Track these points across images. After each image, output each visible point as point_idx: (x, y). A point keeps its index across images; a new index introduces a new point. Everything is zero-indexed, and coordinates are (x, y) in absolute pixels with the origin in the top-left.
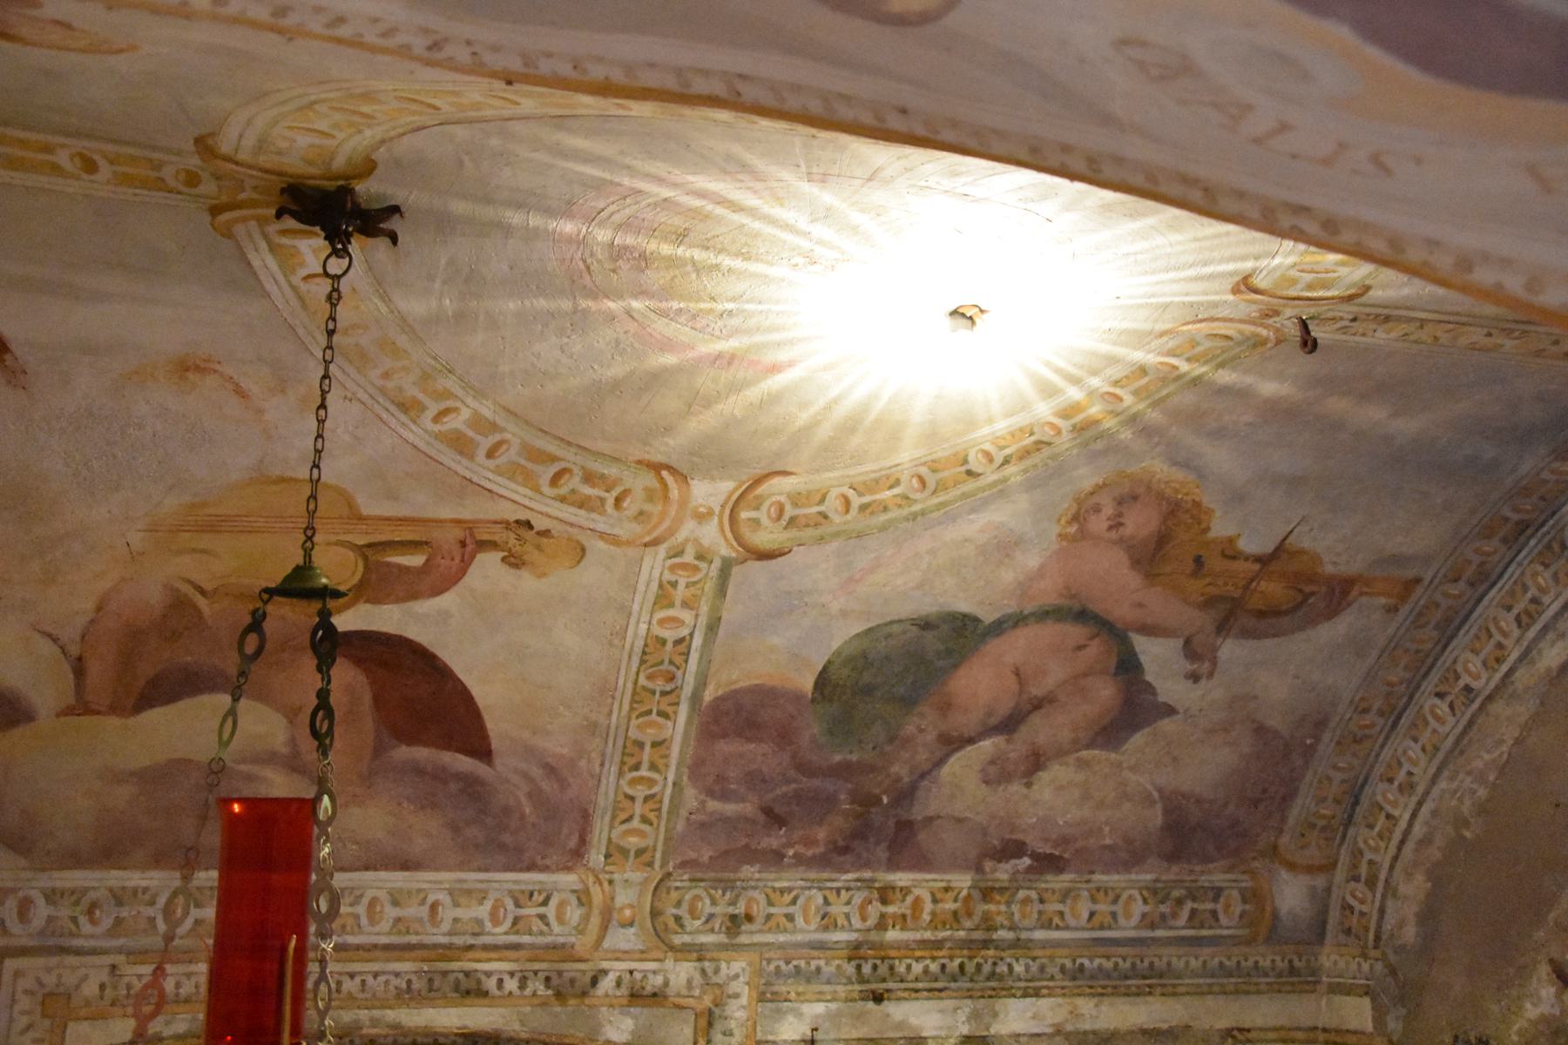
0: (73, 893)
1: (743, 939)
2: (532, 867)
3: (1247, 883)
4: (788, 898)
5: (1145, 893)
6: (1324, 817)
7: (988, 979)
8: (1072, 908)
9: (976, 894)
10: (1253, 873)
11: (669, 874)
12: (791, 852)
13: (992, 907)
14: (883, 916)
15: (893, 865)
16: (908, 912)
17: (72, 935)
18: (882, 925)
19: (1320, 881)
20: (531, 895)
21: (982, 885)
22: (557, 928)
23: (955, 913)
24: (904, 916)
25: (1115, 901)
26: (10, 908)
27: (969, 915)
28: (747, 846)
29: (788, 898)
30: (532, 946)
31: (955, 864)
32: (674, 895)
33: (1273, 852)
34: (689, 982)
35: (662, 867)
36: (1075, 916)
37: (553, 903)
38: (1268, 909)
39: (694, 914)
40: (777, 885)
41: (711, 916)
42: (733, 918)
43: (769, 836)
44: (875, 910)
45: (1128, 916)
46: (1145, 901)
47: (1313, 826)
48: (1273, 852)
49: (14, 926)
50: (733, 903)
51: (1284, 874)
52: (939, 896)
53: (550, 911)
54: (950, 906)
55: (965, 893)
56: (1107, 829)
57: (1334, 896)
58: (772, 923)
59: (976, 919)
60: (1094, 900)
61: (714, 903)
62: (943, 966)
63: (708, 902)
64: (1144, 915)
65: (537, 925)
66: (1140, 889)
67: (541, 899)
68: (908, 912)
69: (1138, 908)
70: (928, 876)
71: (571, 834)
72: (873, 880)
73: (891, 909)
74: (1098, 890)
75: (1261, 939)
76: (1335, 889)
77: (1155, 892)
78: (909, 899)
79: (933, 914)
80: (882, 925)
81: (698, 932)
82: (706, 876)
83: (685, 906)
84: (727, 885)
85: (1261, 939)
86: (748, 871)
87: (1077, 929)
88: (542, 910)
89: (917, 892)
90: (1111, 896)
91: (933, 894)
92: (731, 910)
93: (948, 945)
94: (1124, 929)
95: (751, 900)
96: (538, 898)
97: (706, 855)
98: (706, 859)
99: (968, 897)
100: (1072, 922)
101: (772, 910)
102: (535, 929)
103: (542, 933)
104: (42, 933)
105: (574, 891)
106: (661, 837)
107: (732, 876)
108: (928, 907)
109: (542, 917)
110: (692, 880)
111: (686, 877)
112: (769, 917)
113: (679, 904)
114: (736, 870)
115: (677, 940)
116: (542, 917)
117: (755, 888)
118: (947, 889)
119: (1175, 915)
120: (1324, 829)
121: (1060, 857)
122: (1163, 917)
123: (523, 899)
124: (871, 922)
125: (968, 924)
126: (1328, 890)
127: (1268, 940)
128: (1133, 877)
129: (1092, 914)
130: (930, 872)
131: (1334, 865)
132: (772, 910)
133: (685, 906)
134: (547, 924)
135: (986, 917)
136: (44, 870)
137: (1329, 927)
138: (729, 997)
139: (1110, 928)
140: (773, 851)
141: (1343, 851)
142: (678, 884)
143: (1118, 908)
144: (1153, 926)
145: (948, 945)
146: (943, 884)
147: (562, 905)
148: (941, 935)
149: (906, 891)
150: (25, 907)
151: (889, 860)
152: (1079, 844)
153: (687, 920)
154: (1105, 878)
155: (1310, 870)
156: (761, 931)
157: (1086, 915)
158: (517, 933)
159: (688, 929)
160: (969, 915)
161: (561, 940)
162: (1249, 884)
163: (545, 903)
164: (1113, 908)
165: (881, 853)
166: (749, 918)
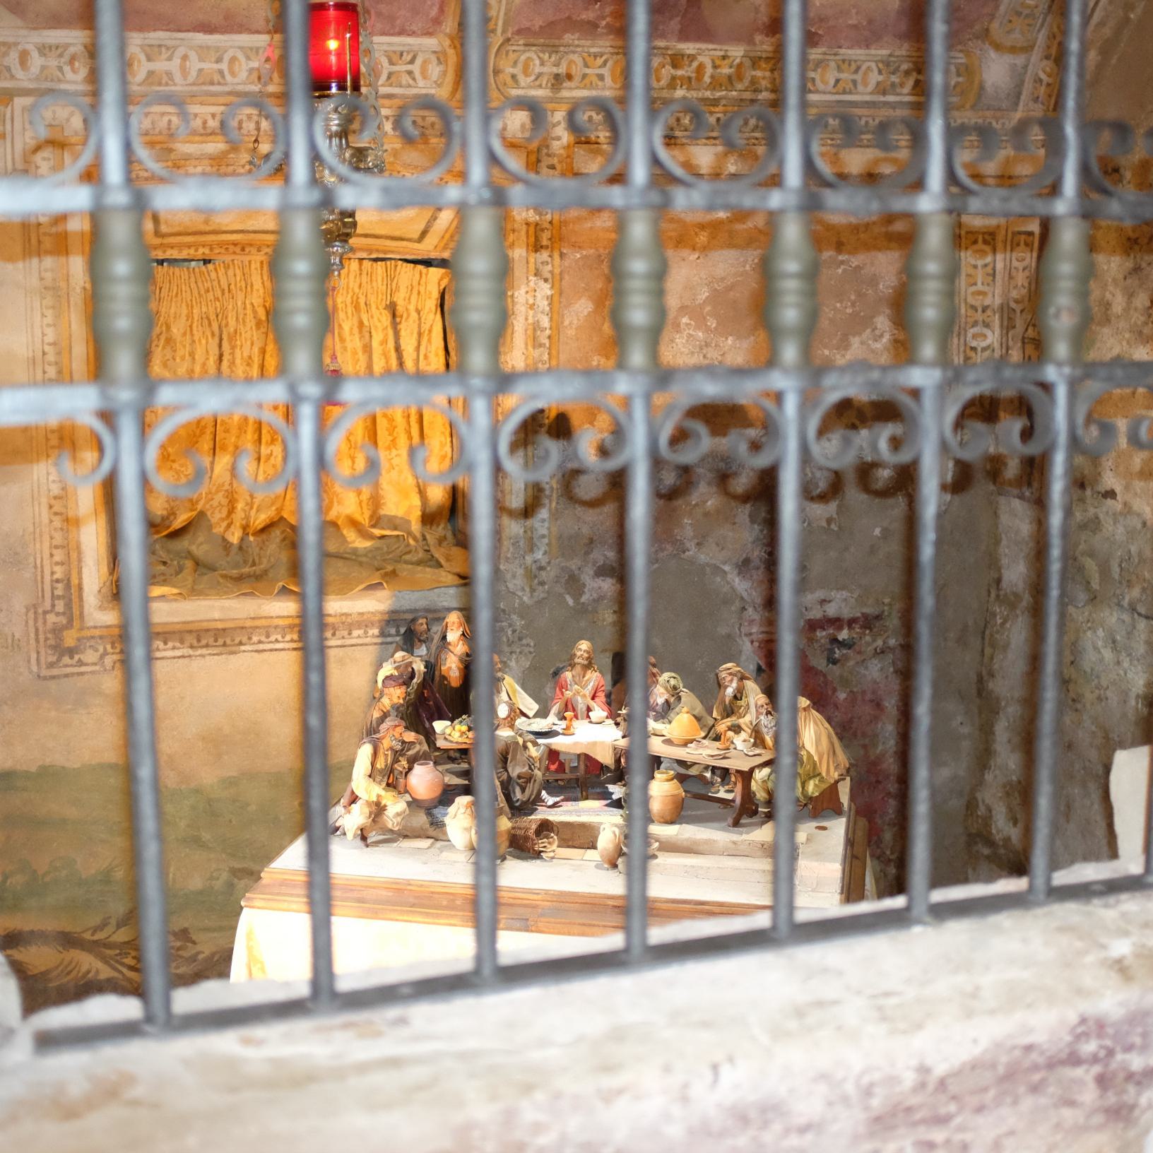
0: (57, 48)
1: (565, 94)
2: (400, 34)
3: (962, 60)
4: (600, 61)
5: (881, 65)
6: (1029, 7)
7: (753, 131)
8: (822, 76)
9: (748, 63)
10: (968, 54)
11: (508, 40)
12: (604, 23)
13: (759, 73)
14: (674, 78)
15: (684, 36)
16: (694, 75)
17: (59, 81)
18: (672, 85)
19: (1020, 60)
20: (401, 55)
21: (752, 54)
22: (421, 83)
23: (730, 78)
24: (690, 78)
25: (856, 71)
26: (13, 58)
27: (740, 78)
28: (569, 18)
29: (600, 61)
30: (403, 96)
31: (736, 39)
32: (512, 56)
33: (985, 34)
34: (523, 126)
35: (504, 32)
36: (825, 83)
37: (419, 61)
38: (976, 82)
39: (526, 72)
40: (592, 50)
41: (539, 75)
42: (557, 76)
43: (587, 9)
44: (667, 71)
45: (866, 85)
46: (880, 72)
47: (1019, 14)
48: (985, 34)
49: (19, 74)
50: (557, 65)
51: (992, 54)
52: (718, 62)
53: (416, 68)
54: (726, 71)
55: (738, 61)
56: (854, 11)
57: (1029, 72)
58: (587, 81)
59: (746, 82)
60: (839, 69)
61: (542, 64)
62: (718, 119)
63: (537, 62)
64: (878, 83)
65: (405, 79)
66: (876, 62)
67: (409, 58)
68: (694, 75)
69: (874, 78)
70: (711, 46)
71: (433, 4)
72: (667, 48)
73: (680, 73)
74: (844, 61)
75: (968, 106)
76: (1030, 67)
77: (888, 64)
78: (695, 64)
79: (712, 77)
80: (672, 85)
81: (530, 87)
82: (536, 42)
83: (520, 66)
84: (554, 49)
85: (968, 106)
86: (568, 38)
87: (824, 93)
88: (409, 67)
89: (700, 59)
90: (854, 66)
91: (713, 61)
92: (555, 70)
93: (723, 102)
94: (863, 94)
95: (571, 62)
96: (408, 57)
97: (538, 22)
98: (537, 28)
99: (740, 66)
100: (821, 86)
101: (588, 71)
102: (404, 82)
103: (409, 86)
104: (37, 79)
105: (435, 52)
106: (503, 8)
107: (557, 42)
108: (709, 70)
109: (410, 73)
110: (525, 45)
111: (521, 42)
112: (584, 76)
113: (515, 63)
114: (560, 38)
115: (515, 92)
116: (410, 73)
117: (574, 52)
118: (724, 58)
119: (902, 85)
120: (1027, 16)
121: (816, 34)
122: (893, 85)
123: (395, 58)
124: (663, 83)
125: (740, 86)
126: (1026, 67)
127: (973, 107)
128: (873, 52)
129: (837, 81)
130: (712, 42)
131: (1032, 47)
132: (588, 71)
133: (520, 66)
134: (414, 79)
135: (754, 81)
136: (35, 29)
137: (1023, 97)
138: (553, 139)
139: (850, 93)
140: (589, 22)
141: (1040, 36)
142: (514, 48)
143: (858, 77)
144: (884, 93)
145: (723, 102)
146: (722, 53)
147: (425, 62)
148: (718, 94)
149: (692, 58)
150: (24, 57)
151: (681, 31)
152: (831, 23)
153: (523, 80)
154: (850, 52)
155: (1013, 50)
156: (577, 88)
157: (832, 82)
158: (391, 85)
159: (523, 84)
160: (740, 78)
161: (424, 91)
162: (963, 61)
163: (412, 62)
164: (855, 77)
165: (675, 24)
166: (569, 77)
